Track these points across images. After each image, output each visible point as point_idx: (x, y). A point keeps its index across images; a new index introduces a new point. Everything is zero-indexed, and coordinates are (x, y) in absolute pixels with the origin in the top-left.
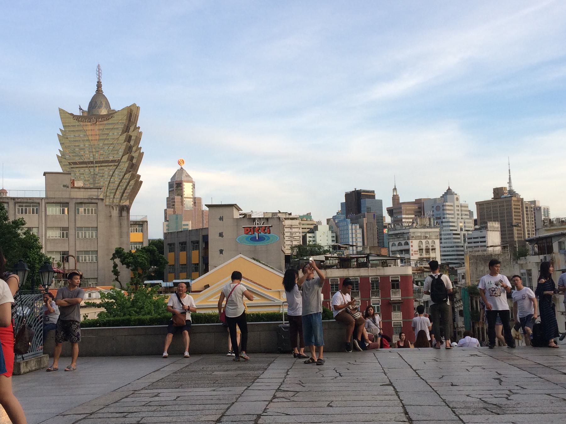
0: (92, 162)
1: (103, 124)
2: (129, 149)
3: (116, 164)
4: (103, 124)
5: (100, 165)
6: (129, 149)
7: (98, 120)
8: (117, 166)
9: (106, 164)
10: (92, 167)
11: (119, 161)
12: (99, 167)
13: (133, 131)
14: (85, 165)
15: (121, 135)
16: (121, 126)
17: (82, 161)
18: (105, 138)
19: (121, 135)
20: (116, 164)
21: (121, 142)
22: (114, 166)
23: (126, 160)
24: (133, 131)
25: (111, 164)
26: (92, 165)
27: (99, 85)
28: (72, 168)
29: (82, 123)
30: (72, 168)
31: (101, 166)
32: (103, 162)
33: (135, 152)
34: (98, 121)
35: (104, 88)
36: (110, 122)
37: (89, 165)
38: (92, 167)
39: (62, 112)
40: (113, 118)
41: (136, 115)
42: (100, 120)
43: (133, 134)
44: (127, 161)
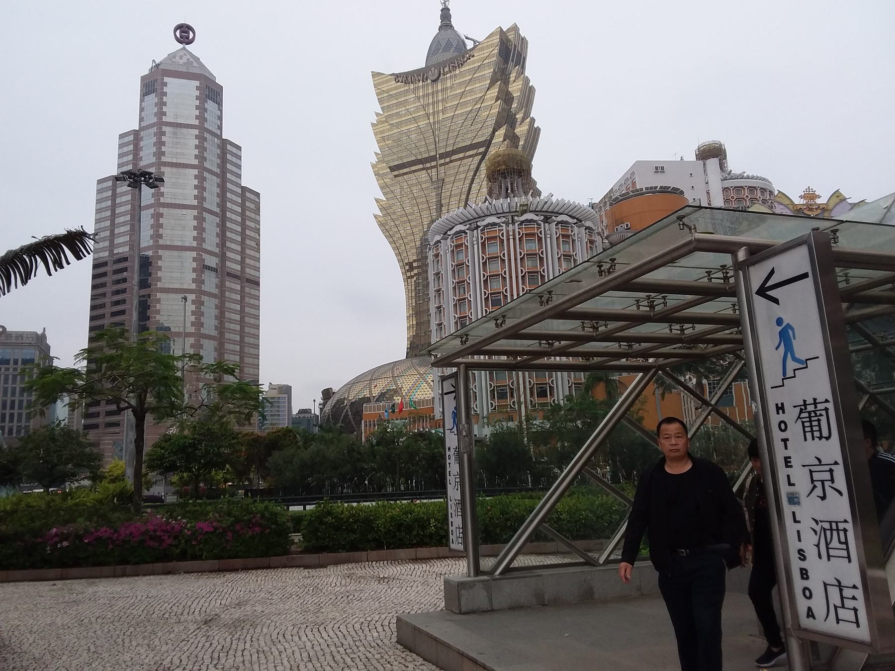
0: (433, 158)
1: (451, 77)
2: (507, 119)
3: (482, 150)
4: (451, 77)
5: (448, 160)
6: (507, 119)
7: (442, 71)
8: (484, 155)
9: (461, 155)
10: (432, 167)
11: (488, 143)
12: (447, 163)
13: (514, 81)
14: (421, 166)
15: (488, 89)
16: (488, 72)
17: (413, 158)
18: (457, 102)
19: (488, 89)
20: (482, 150)
21: (489, 103)
22: (476, 155)
23: (502, 139)
24: (514, 81)
25: (471, 153)
26: (433, 164)
27: (446, 15)
28: (396, 176)
29: (412, 86)
30: (396, 176)
31: (451, 161)
32: (454, 152)
33: (522, 121)
34: (442, 72)
35: (454, 22)
36: (467, 68)
37: (428, 165)
38: (432, 167)
39: (375, 75)
40: (472, 59)
41: (519, 55)
42: (447, 69)
43: (515, 88)
44: (504, 140)
